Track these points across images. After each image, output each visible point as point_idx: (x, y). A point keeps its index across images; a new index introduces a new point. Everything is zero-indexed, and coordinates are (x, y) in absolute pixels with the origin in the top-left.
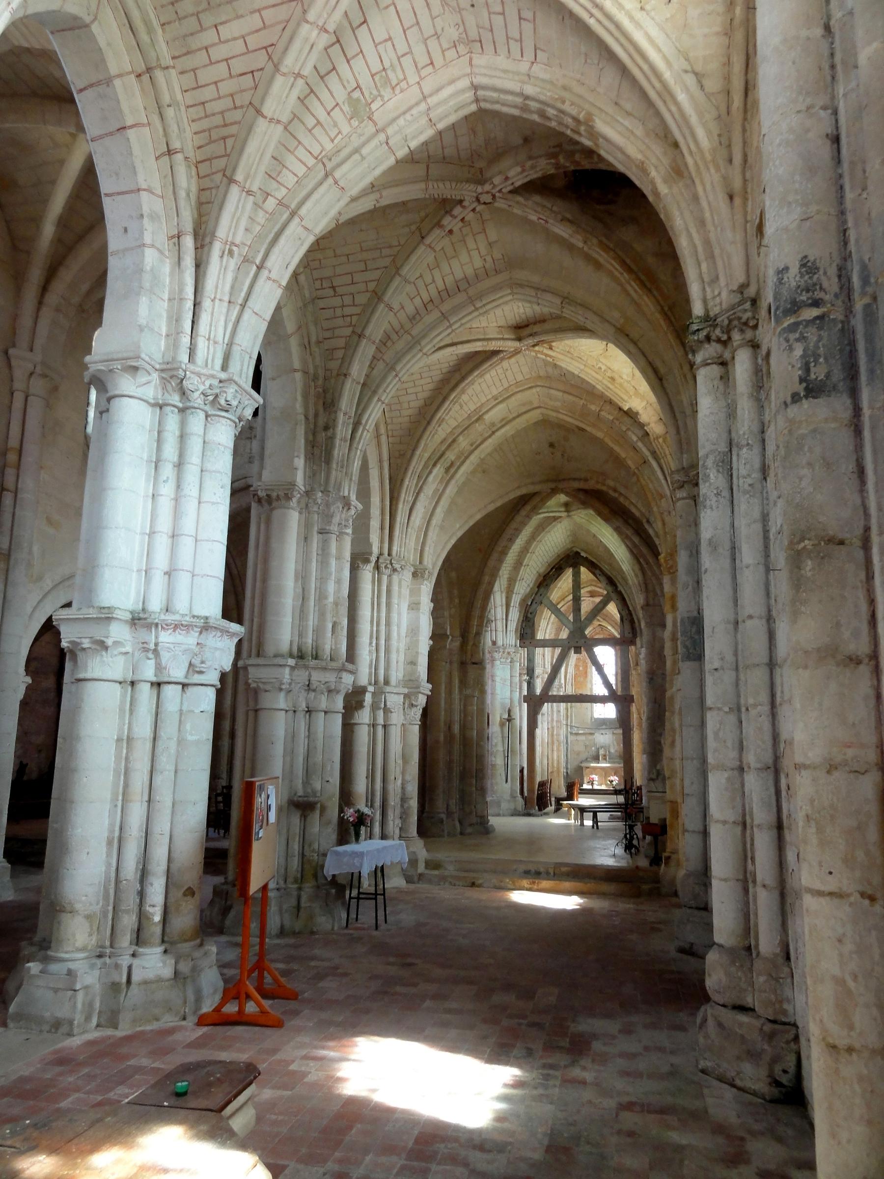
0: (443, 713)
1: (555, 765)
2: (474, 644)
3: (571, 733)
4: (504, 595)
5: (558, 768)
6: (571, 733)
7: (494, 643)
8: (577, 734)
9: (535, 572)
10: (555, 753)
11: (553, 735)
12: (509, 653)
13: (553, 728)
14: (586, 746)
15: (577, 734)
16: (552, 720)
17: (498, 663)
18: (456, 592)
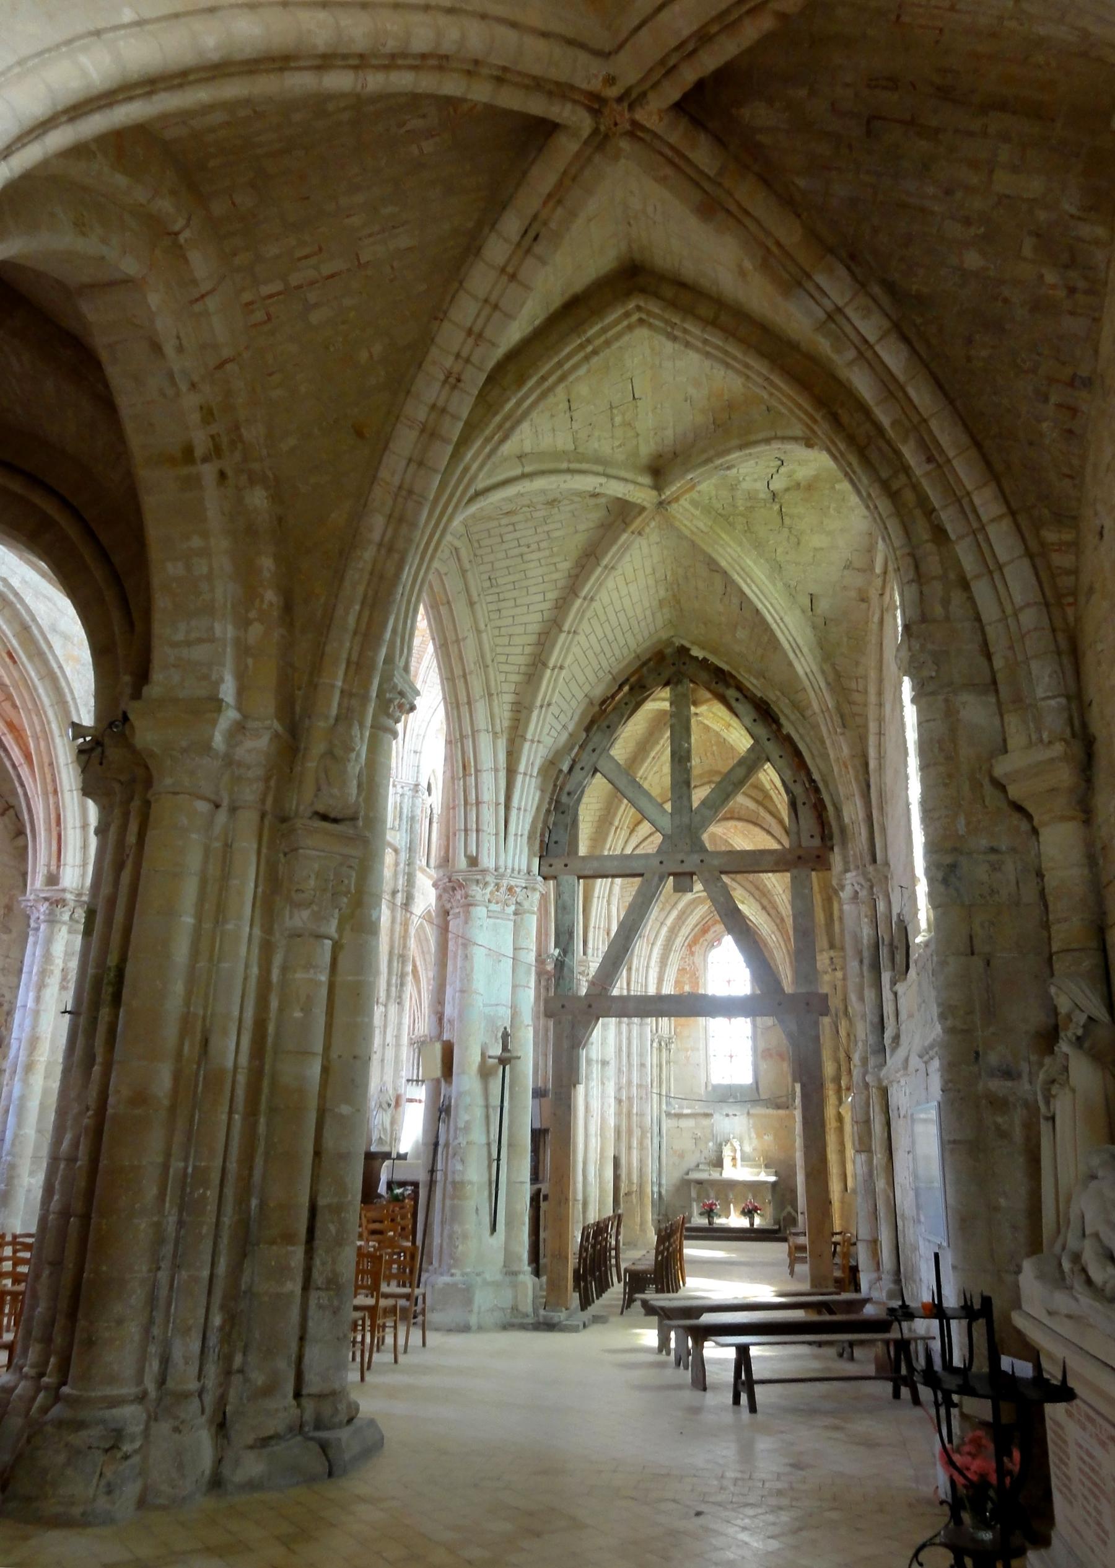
0: (178, 987)
1: (635, 1179)
2: (330, 754)
3: (668, 1114)
4: (502, 744)
5: (641, 1185)
6: (668, 1114)
7: (473, 861)
8: (679, 1116)
9: (580, 695)
10: (635, 1153)
11: (629, 1114)
12: (510, 889)
13: (630, 1099)
14: (697, 1140)
15: (679, 1116)
16: (629, 1083)
17: (480, 912)
18: (267, 564)
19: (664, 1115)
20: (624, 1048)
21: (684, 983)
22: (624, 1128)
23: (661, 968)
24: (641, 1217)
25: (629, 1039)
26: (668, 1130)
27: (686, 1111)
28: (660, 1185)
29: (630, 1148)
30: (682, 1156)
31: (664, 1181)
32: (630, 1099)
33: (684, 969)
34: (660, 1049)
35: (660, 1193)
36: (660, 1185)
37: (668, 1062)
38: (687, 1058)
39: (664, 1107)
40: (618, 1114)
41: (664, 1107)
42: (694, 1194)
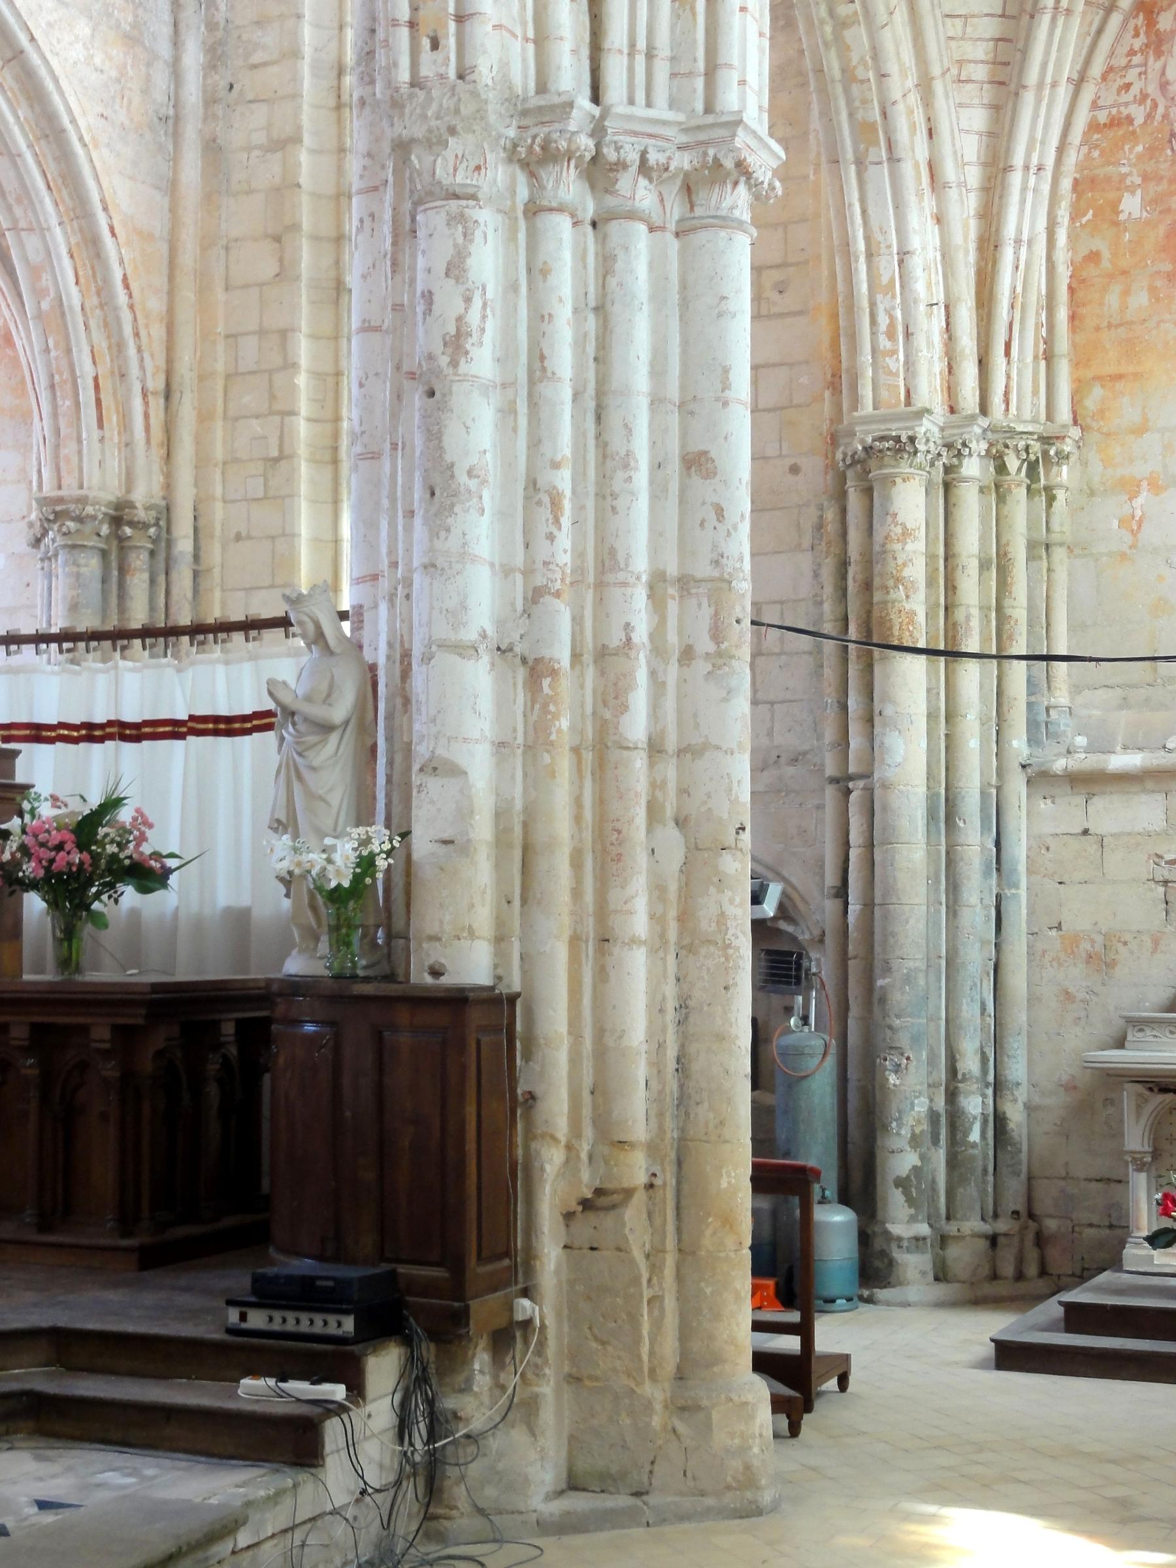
3: (1040, 779)
5: (684, 1156)
6: (1040, 779)
8: (1089, 782)
10: (638, 977)
11: (601, 750)
15: (1089, 782)
16: (605, 565)
19: (1017, 785)
20: (564, 360)
21: (1121, 185)
22: (561, 827)
23: (996, 108)
24: (685, 1334)
25: (602, 309)
26: (1040, 845)
27: (1121, 761)
28: (999, 1087)
29: (601, 940)
30: (1102, 961)
31: (1017, 1070)
32: (605, 657)
33: (1114, 122)
34: (999, 491)
35: (1000, 1121)
36: (999, 1087)
37: (1040, 548)
38: (1133, 525)
39: (1018, 744)
40: (528, 746)
41: (1018, 744)
42: (1136, 1139)
